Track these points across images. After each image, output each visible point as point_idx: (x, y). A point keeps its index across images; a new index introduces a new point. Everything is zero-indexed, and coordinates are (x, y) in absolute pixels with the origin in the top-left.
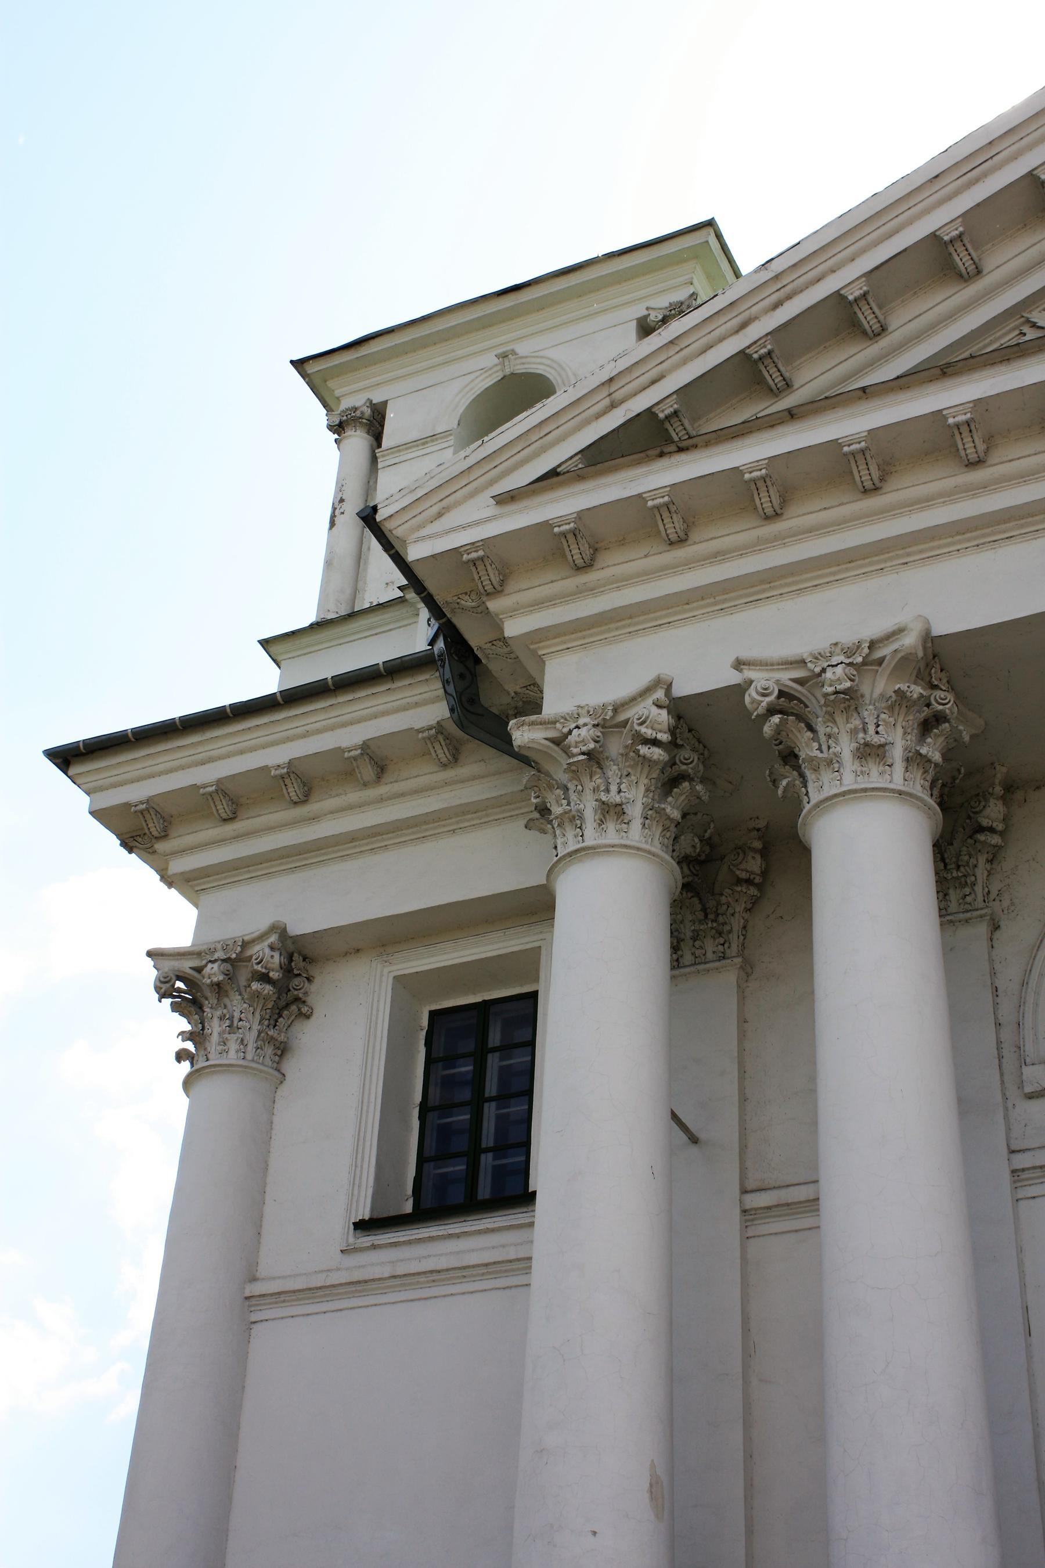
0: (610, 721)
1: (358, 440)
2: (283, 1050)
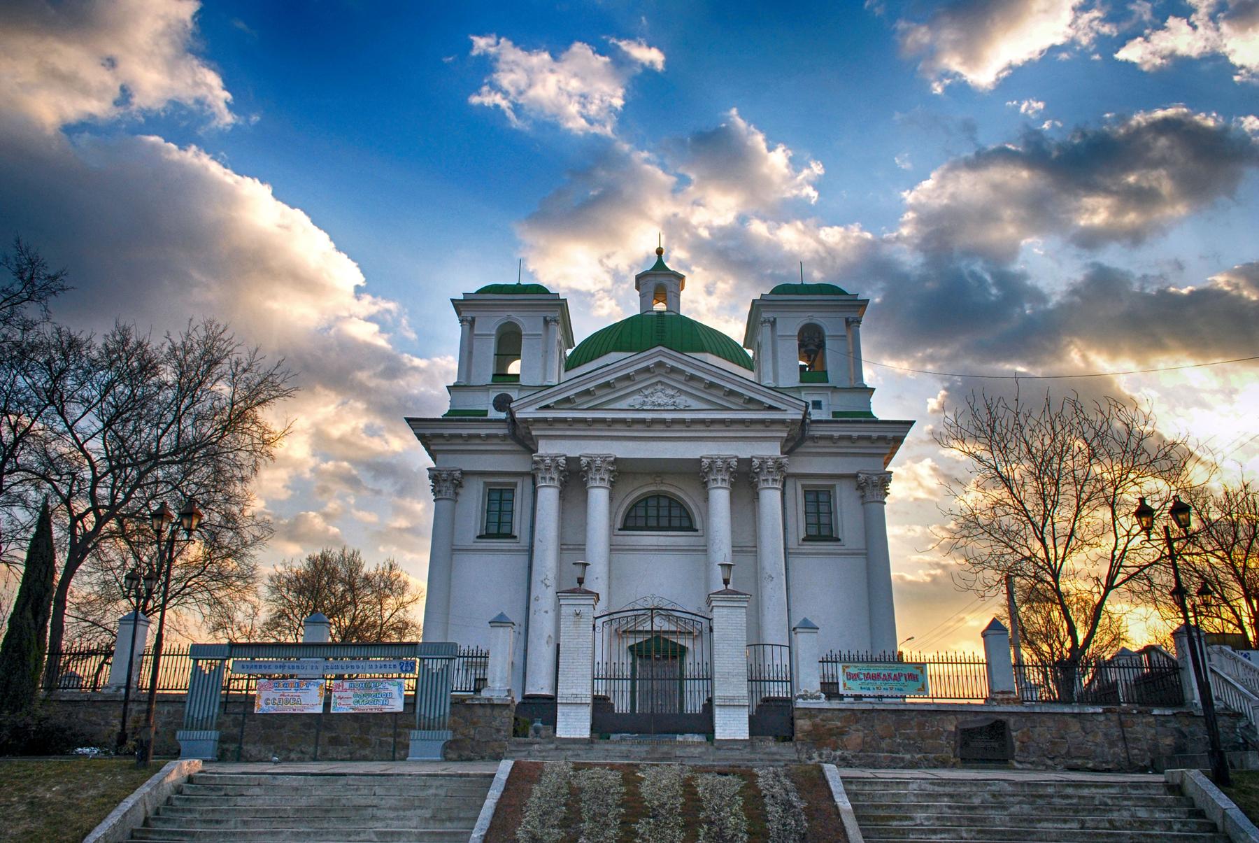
0: (554, 459)
1: (467, 327)
2: (457, 494)
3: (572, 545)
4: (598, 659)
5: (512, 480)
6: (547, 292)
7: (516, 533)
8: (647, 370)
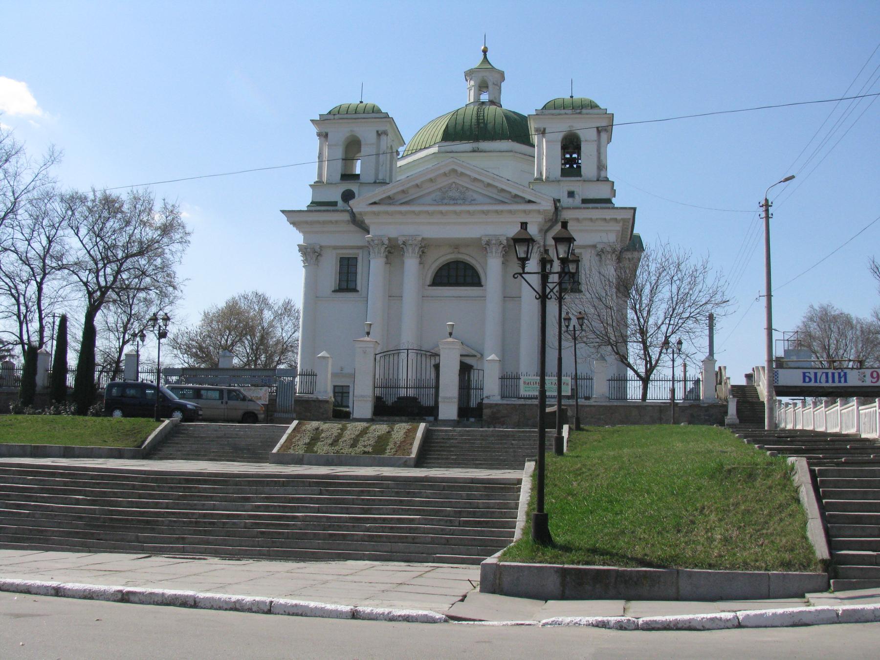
3: (393, 296)
4: (377, 376)
5: (356, 251)
6: (379, 111)
7: (359, 288)
8: (445, 174)
